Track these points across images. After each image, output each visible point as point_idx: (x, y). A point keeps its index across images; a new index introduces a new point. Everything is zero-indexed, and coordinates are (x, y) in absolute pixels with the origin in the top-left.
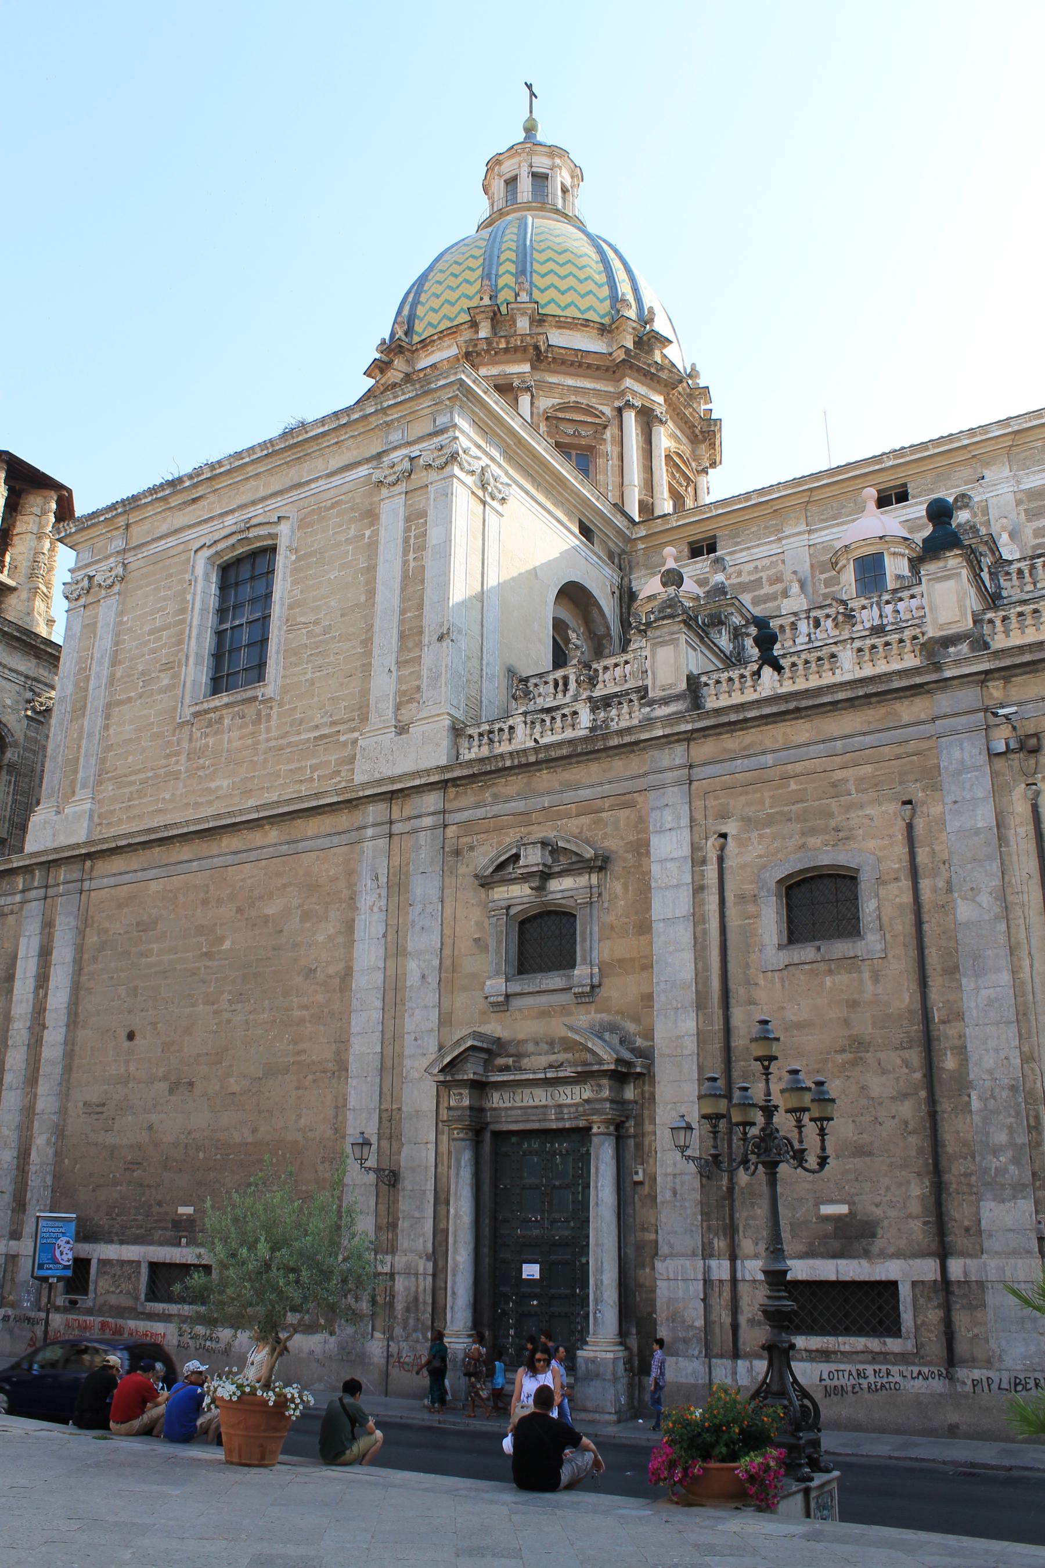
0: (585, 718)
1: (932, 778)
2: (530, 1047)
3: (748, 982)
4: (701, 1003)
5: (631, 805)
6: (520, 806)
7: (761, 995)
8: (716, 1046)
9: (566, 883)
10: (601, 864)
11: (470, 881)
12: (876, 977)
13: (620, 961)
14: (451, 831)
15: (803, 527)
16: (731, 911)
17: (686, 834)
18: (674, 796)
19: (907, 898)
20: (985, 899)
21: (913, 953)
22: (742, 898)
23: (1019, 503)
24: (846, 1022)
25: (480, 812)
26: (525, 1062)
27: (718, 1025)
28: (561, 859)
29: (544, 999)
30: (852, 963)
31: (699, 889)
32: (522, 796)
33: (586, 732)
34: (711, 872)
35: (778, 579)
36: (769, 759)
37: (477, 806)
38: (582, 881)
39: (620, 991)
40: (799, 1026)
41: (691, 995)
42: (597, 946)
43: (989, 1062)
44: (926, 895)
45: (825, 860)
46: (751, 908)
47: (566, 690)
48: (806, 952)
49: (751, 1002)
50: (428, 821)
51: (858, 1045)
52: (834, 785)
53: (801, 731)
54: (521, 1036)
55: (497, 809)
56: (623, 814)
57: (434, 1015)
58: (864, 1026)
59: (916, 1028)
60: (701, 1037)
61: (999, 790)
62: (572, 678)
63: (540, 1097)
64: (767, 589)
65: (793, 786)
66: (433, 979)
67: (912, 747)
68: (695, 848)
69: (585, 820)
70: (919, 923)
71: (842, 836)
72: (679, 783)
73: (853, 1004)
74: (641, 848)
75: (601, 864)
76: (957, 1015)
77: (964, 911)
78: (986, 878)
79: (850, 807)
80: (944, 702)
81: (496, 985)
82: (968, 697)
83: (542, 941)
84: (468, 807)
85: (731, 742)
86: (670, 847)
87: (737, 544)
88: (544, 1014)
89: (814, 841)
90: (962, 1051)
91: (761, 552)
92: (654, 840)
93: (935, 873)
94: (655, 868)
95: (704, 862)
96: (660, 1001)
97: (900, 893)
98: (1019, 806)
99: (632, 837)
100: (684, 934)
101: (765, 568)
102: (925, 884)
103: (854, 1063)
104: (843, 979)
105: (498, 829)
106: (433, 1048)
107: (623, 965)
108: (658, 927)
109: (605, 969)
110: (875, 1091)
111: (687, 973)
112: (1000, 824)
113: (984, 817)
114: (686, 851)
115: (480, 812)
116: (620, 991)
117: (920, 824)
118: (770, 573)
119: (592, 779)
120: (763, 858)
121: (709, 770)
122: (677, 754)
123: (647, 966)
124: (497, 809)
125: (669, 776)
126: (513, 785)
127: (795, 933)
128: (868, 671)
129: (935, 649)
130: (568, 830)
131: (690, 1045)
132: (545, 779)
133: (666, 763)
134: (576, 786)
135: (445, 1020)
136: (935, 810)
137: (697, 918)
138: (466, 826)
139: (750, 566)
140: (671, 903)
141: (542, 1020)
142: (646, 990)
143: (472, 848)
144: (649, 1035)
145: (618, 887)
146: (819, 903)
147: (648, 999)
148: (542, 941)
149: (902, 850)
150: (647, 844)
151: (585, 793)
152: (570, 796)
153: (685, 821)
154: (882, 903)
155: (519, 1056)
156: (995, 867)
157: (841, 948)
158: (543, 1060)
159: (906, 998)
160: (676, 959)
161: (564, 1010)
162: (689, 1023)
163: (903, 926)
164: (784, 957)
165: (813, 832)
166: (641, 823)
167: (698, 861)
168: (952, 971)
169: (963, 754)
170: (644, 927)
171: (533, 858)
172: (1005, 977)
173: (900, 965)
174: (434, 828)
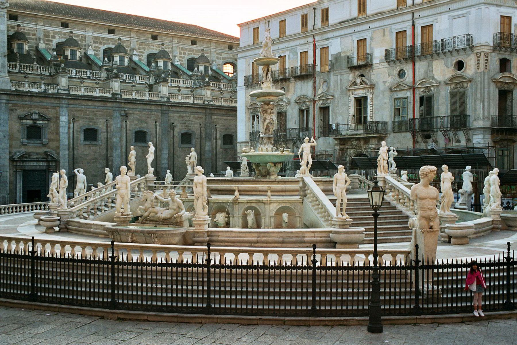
0: (43, 87)
1: (111, 117)
2: (32, 154)
3: (78, 146)
4: (69, 149)
5: (54, 109)
6: (29, 103)
7: (80, 149)
8: (71, 157)
9: (41, 122)
10: (48, 120)
11: (16, 117)
12: (100, 148)
13: (52, 139)
14: (10, 105)
15: (42, 24)
16: (75, 133)
17: (67, 117)
18: (65, 109)
19: (106, 136)
20: (118, 138)
21: (106, 145)
22: (77, 131)
23: (92, 38)
24: (94, 155)
25: (19, 102)
26: (32, 157)
27: (71, 153)
28: (42, 117)
29: (35, 144)
30: (96, 145)
31: (69, 128)
32: (29, 101)
33: (43, 91)
34: (71, 126)
35: (34, 35)
36: (84, 107)
37: (18, 101)
38: (44, 122)
39: (53, 145)
40: (86, 155)
41: (67, 148)
42: (47, 135)
43: (116, 163)
44: (109, 136)
45: (93, 127)
46: (79, 133)
47: (16, 68)
48: (88, 143)
49: (78, 150)
50: (4, 101)
51: (96, 159)
52: (95, 114)
53: (90, 103)
54: (30, 151)
55: (23, 103)
56: (53, 110)
57: (8, 145)
58: (97, 156)
59: (105, 157)
60: (69, 155)
61: (122, 121)
62: (18, 65)
63: (35, 164)
64: (31, 36)
65: (88, 113)
66: (7, 138)
67: (108, 111)
68: (69, 120)
69: (45, 110)
70: (107, 141)
71: (95, 123)
72: (66, 107)
73: (96, 152)
74: (57, 118)
75: (48, 120)
76: (112, 156)
77: (115, 140)
78: (118, 135)
79: (97, 119)
80: (115, 105)
81: (25, 141)
82: (118, 105)
83: (34, 132)
84: (16, 100)
85: (77, 102)
86: (64, 119)
87: (24, 21)
88: (35, 147)
89: (91, 123)
90: (112, 161)
91: (31, 26)
92: (61, 117)
93: (110, 133)
94: (61, 123)
95: (70, 123)
96: (61, 148)
97: (104, 135)
98: (124, 125)
99: (55, 115)
100: (66, 136)
101: (31, 30)
102: (109, 134)
103: (95, 162)
104: (94, 148)
105: (23, 107)
106: (7, 152)
107: (52, 140)
108: (61, 134)
109: (50, 140)
110: (98, 166)
111: (67, 143)
112: (121, 127)
113: (119, 125)
114: (67, 120)
115: (19, 102)
116: (53, 145)
117: (109, 124)
118: (33, 32)
119: (48, 102)
120: (82, 124)
121: (72, 106)
122: (66, 101)
123: (58, 141)
124: (23, 103)
125: (64, 105)
126: (27, 99)
127: (85, 139)
128: (101, 94)
129: (114, 94)
130: (42, 110)
131: (67, 156)
132: (35, 99)
133: (64, 102)
134: (43, 102)
135: (11, 146)
136: (111, 122)
137: (68, 133)
138: (15, 105)
139: (28, 28)
140: (63, 130)
141: (34, 148)
142: (57, 145)
143: (16, 110)
144: (58, 154)
145: (52, 124)
146: (91, 134)
147: (58, 147)
148: (34, 132)
149: (105, 128)
150: (59, 117)
151: (45, 104)
152: (41, 104)
153: (67, 115)
154: (101, 136)
155: (29, 155)
156: (120, 134)
157: (94, 143)
158: (35, 157)
159: (104, 152)
160: (64, 140)
161: (40, 147)
162: (67, 152)
163: (104, 141)
164: (85, 143)
165: (91, 122)
166: (57, 113)
167: (69, 123)
168: (112, 149)
169: (117, 114)
170: (58, 133)
171: (36, 116)
172: (120, 151)
173: (103, 146)
174: (6, 103)
